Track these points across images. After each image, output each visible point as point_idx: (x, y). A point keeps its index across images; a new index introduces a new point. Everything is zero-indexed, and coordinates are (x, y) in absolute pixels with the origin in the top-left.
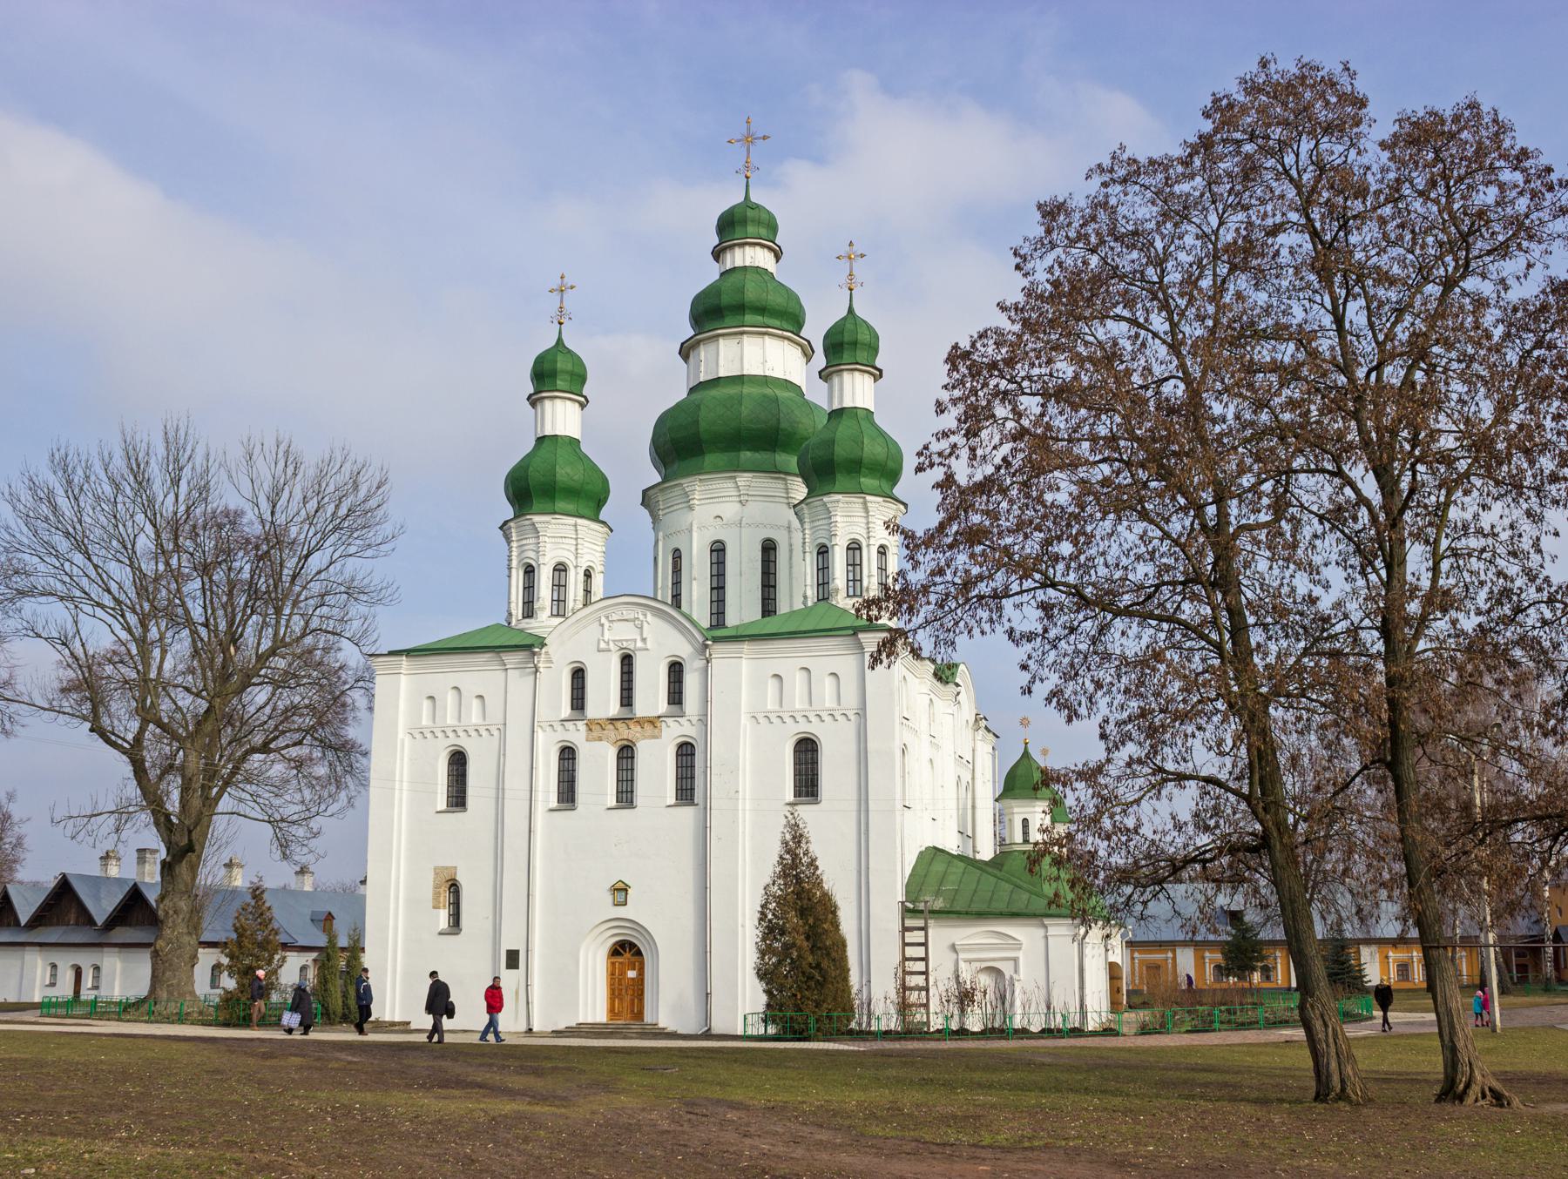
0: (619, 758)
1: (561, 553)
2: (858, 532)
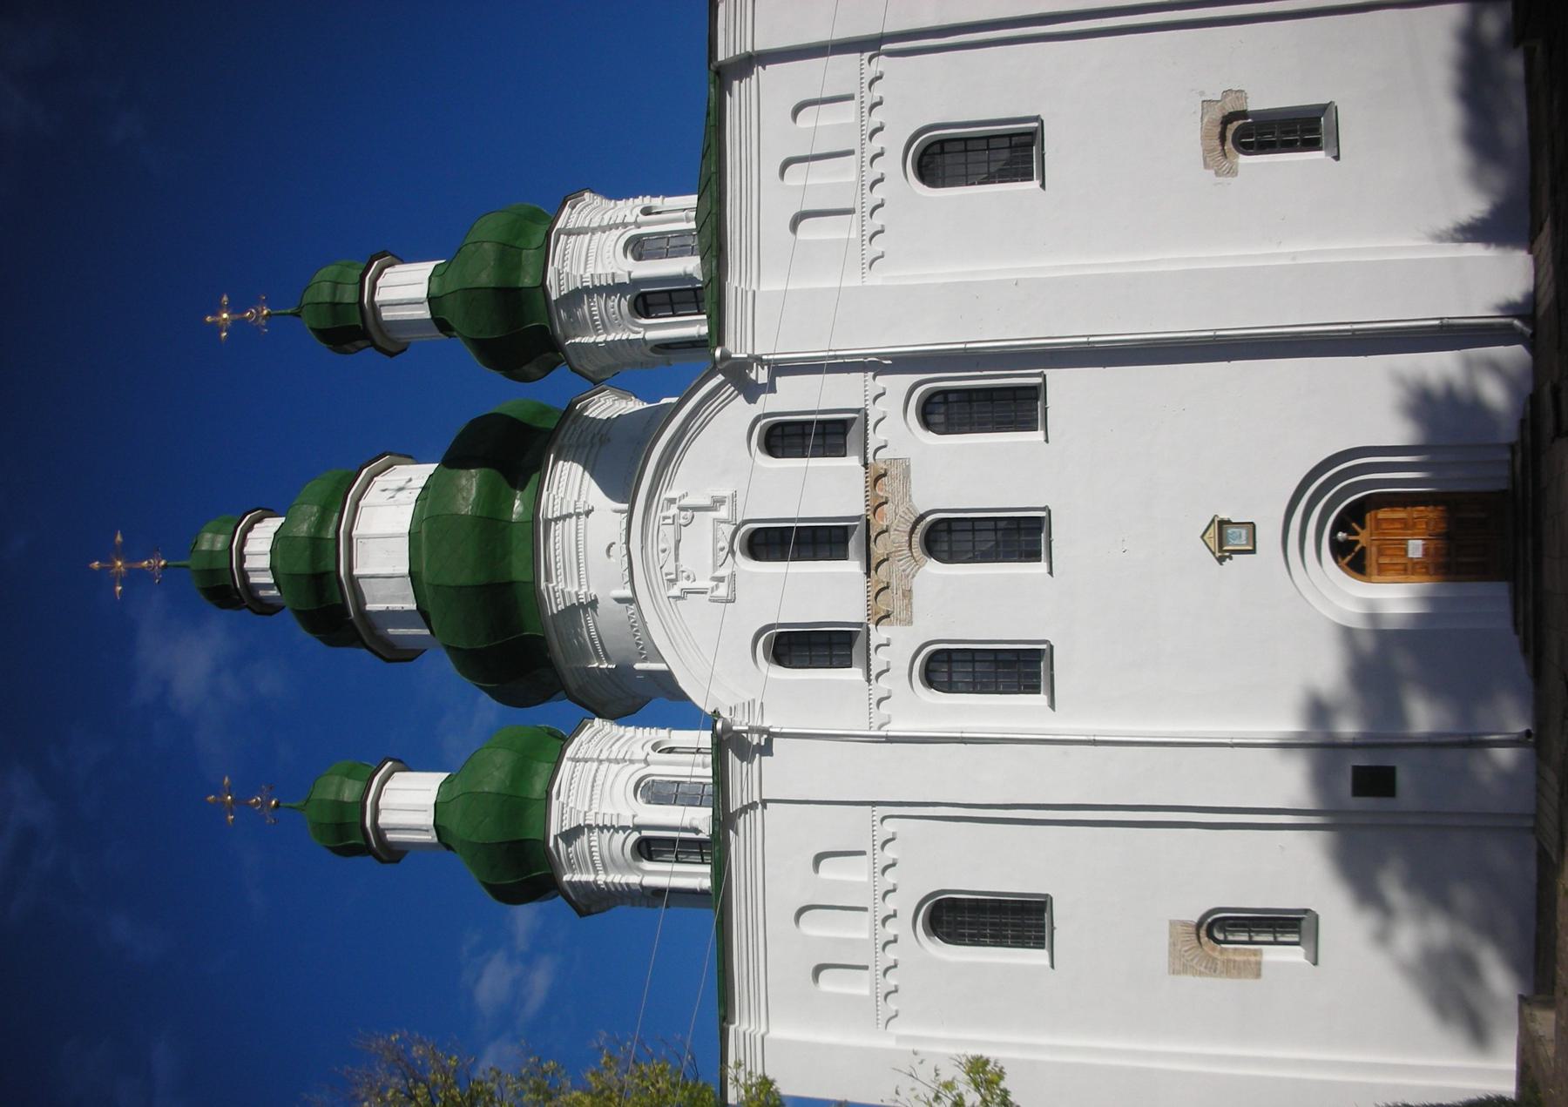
0: (950, 557)
2: (613, 242)
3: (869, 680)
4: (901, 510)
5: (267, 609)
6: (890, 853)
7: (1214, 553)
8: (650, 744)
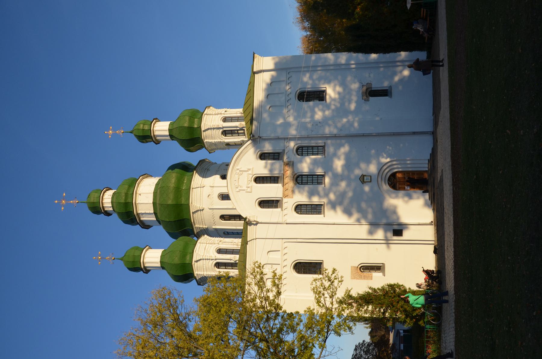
5: (108, 214)
6: (285, 251)
7: (362, 182)
8: (219, 241)
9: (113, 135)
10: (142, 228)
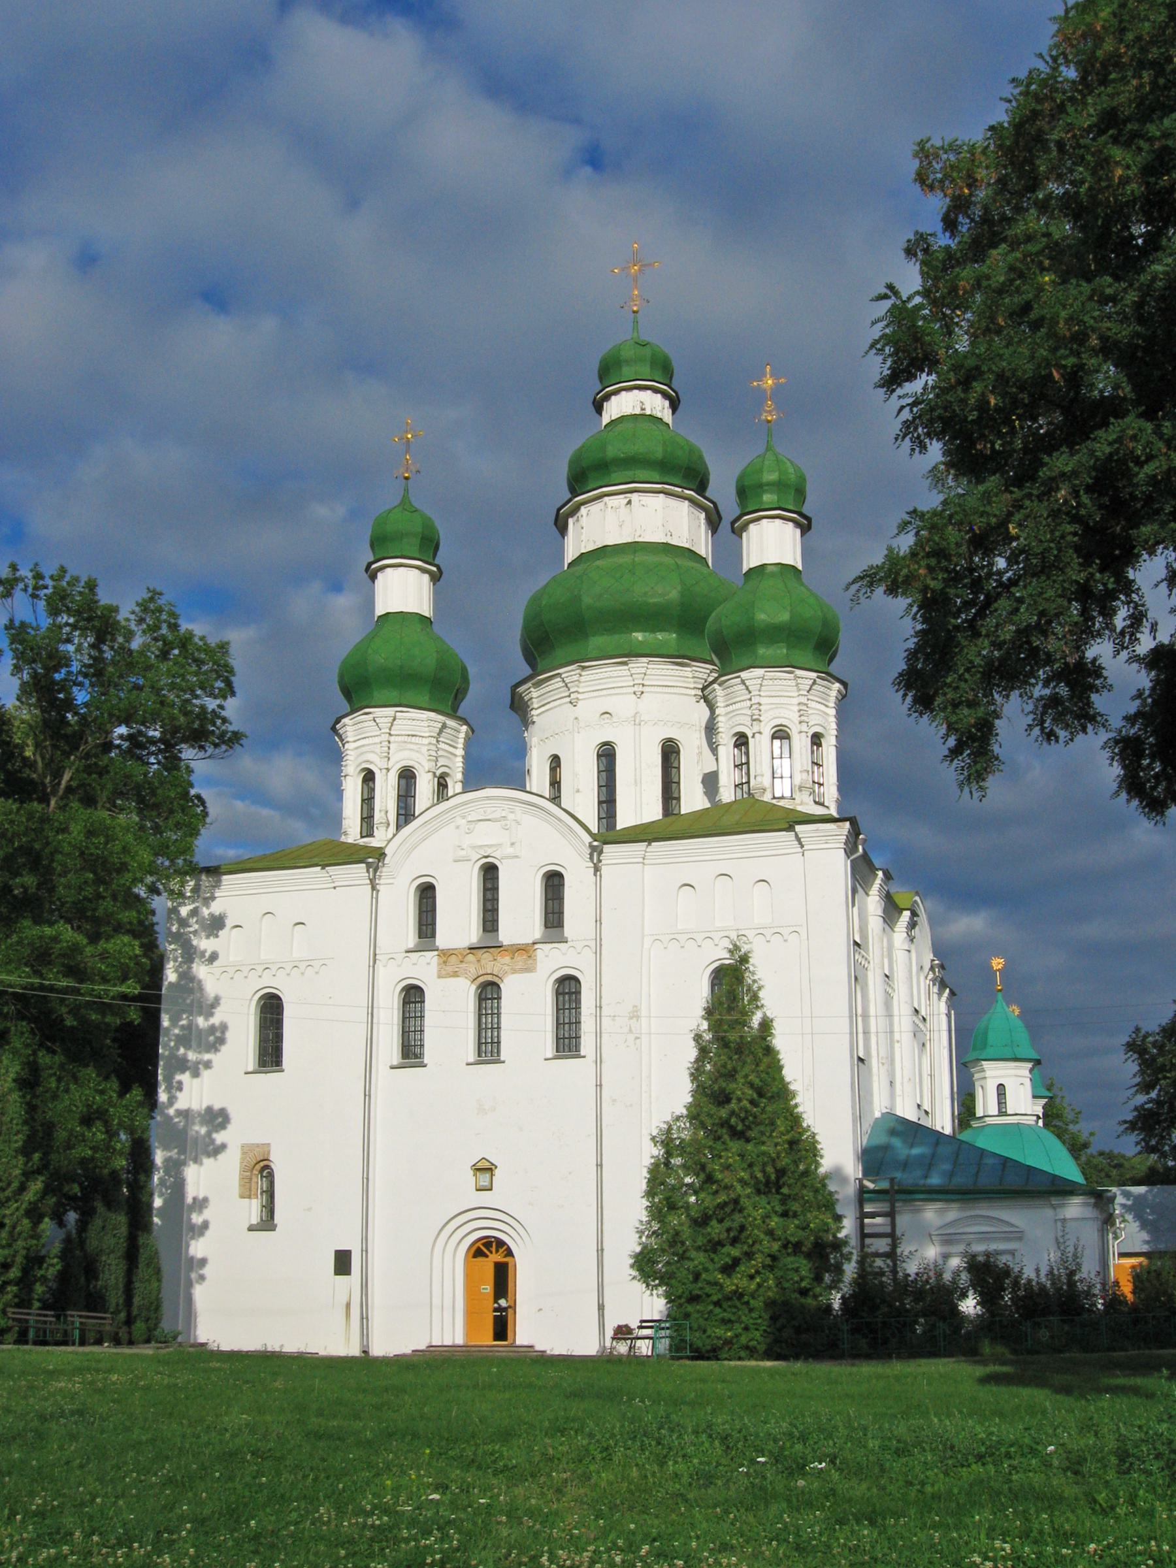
1: (406, 754)
3: (407, 952)
4: (506, 968)
9: (761, 392)
10: (556, 524)
